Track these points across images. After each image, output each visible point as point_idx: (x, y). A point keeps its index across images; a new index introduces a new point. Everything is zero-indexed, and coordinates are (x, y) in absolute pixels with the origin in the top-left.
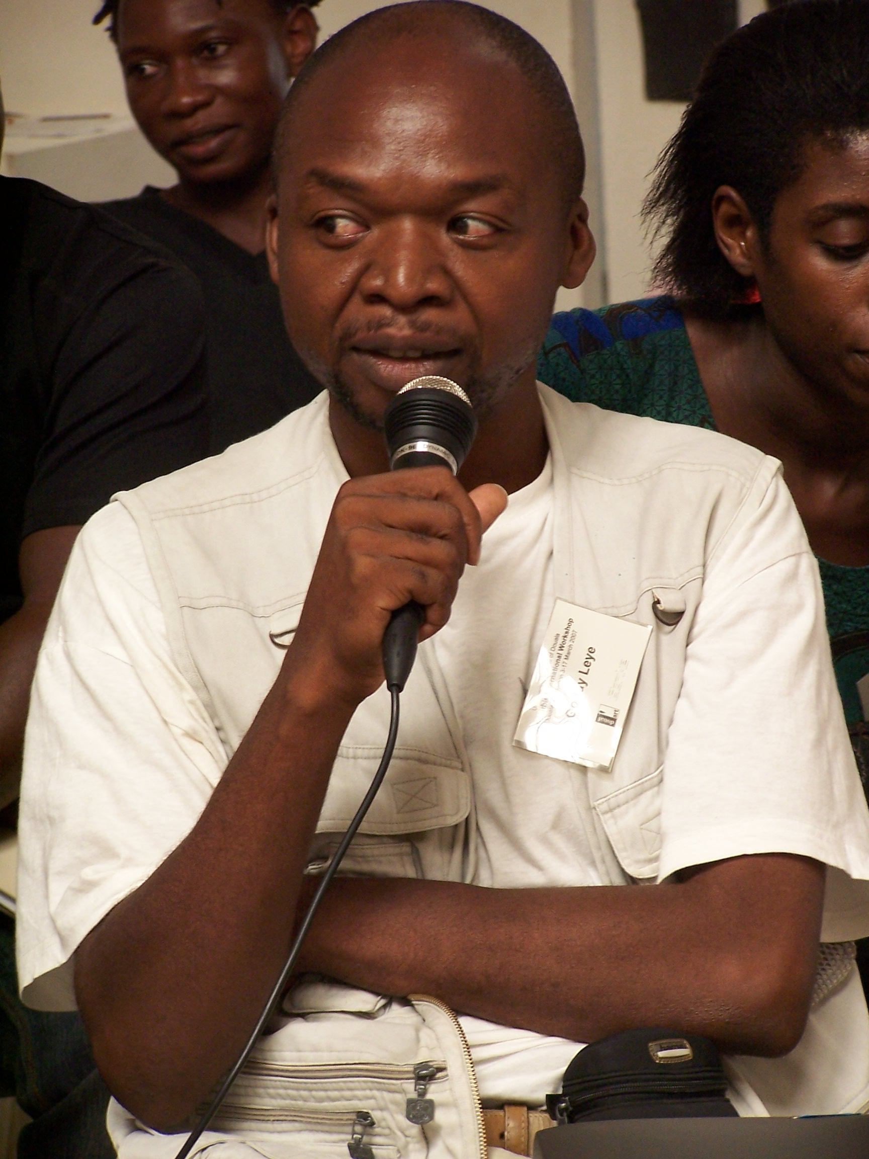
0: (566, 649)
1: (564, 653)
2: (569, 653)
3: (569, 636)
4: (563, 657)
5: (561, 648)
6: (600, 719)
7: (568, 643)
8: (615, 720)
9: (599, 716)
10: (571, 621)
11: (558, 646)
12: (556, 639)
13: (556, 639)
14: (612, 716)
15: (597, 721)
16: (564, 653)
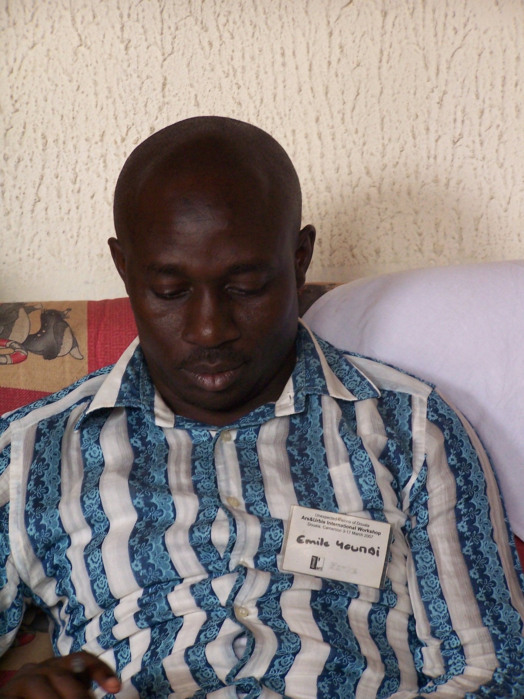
0: (359, 532)
1: (357, 531)
2: (357, 534)
3: (369, 534)
4: (354, 531)
5: (360, 529)
6: (315, 559)
7: (364, 533)
8: (315, 568)
9: (317, 558)
10: (379, 534)
11: (361, 527)
12: (366, 525)
13: (366, 525)
14: (317, 566)
15: (313, 556)
16: (357, 531)
